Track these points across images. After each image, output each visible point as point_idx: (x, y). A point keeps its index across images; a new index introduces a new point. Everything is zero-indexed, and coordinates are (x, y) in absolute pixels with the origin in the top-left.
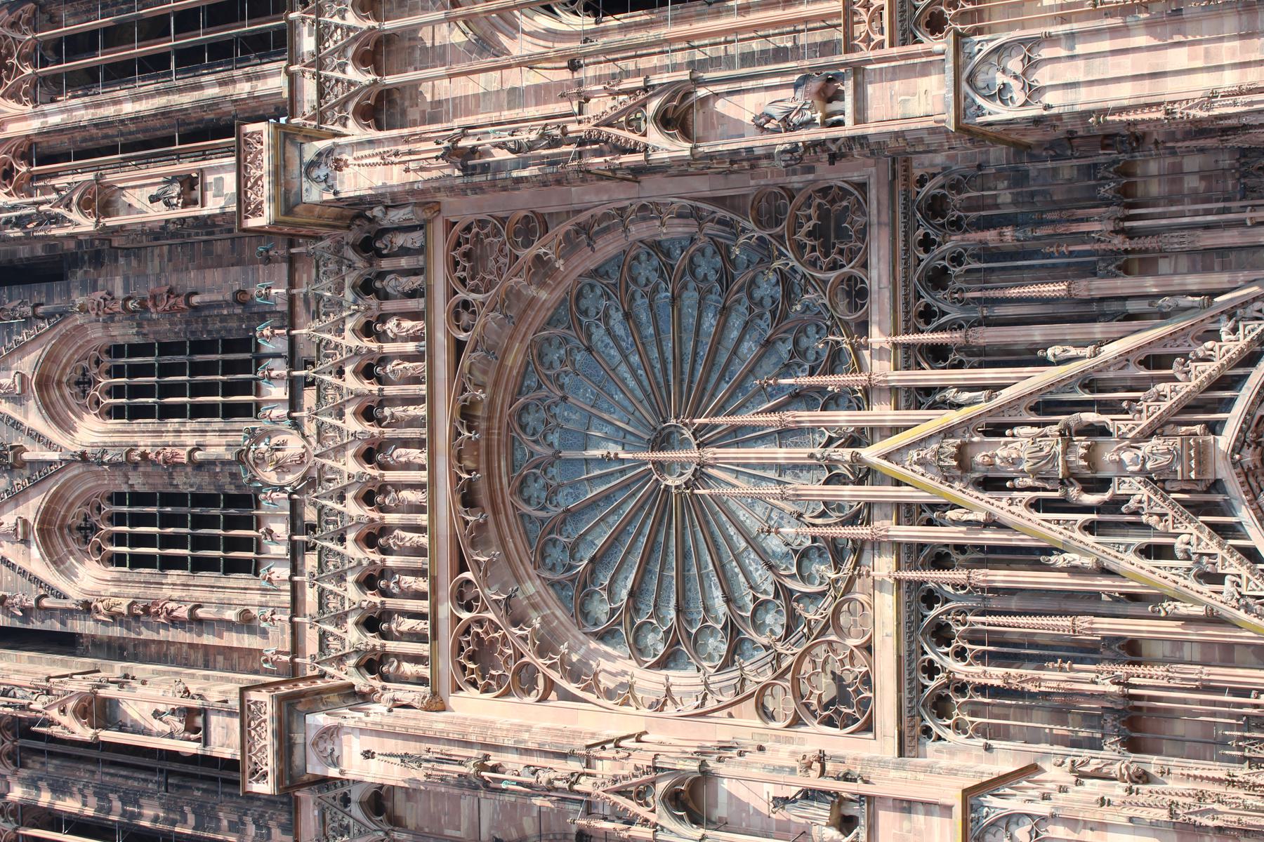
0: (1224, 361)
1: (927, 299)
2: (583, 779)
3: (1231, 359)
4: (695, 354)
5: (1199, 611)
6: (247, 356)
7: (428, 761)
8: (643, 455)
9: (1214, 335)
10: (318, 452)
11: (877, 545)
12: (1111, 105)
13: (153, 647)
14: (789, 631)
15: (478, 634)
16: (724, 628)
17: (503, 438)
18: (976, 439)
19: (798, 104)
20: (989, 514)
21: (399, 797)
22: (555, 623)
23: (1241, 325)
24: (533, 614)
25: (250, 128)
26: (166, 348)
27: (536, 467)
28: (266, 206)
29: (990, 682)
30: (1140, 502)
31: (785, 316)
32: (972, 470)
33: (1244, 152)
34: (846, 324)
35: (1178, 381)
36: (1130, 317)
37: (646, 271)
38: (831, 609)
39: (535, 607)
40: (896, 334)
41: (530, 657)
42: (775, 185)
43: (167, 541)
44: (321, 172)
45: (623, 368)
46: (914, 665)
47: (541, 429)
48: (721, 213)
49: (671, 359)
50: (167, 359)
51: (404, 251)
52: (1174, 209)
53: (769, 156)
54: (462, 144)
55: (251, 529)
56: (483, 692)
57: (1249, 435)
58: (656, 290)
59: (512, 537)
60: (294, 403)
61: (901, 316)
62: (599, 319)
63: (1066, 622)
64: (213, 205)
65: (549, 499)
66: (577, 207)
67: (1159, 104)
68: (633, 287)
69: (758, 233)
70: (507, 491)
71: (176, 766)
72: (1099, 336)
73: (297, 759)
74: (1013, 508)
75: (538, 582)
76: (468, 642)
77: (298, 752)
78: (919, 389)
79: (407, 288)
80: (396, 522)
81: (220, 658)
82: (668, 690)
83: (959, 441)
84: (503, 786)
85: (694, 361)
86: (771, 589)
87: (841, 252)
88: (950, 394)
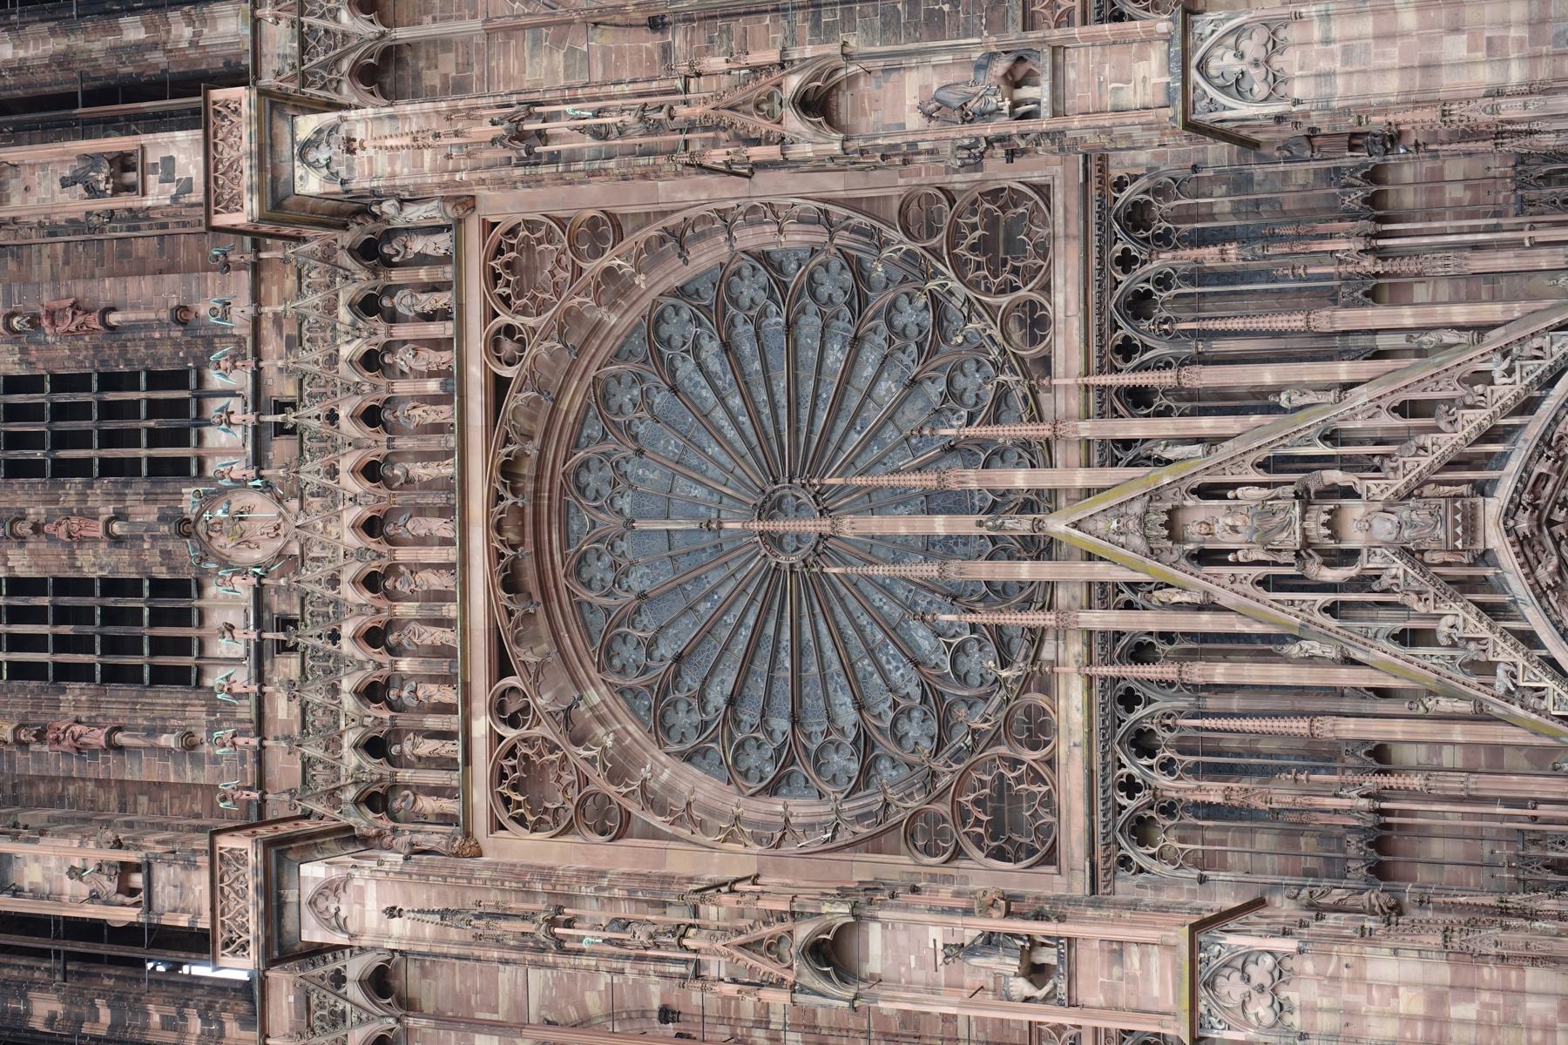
0: (1496, 408)
1: (1126, 330)
2: (692, 932)
3: (1504, 406)
4: (816, 396)
5: (1464, 707)
6: (185, 394)
7: (479, 917)
8: (757, 526)
10: (299, 523)
11: (1061, 633)
12: (1373, 101)
13: (42, 789)
14: (939, 748)
15: (526, 757)
16: (855, 743)
17: (556, 504)
20: (1207, 593)
21: (413, 970)
22: (628, 740)
23: (1517, 364)
24: (600, 731)
25: (218, 94)
26: (62, 383)
28: (246, 197)
29: (1207, 799)
30: (1395, 577)
31: (934, 350)
32: (1185, 541)
33: (1521, 159)
34: (1020, 359)
35: (1442, 431)
36: (1379, 355)
37: (750, 289)
38: (1002, 715)
39: (601, 720)
40: (1087, 374)
41: (600, 783)
43: (62, 644)
44: (322, 155)
45: (719, 415)
46: (1109, 781)
47: (606, 491)
48: (859, 219)
49: (784, 402)
50: (63, 398)
51: (422, 260)
52: (1436, 225)
53: (930, 152)
54: (529, 126)
55: (189, 625)
56: (534, 830)
57: (1525, 496)
58: (763, 313)
59: (568, 631)
60: (258, 460)
61: (1094, 351)
62: (687, 351)
63: (1300, 726)
64: (157, 194)
65: (617, 582)
68: (732, 310)
69: (909, 245)
70: (560, 572)
71: (80, 947)
73: (289, 923)
74: (1236, 586)
75: (603, 689)
76: (514, 768)
79: (428, 308)
80: (413, 612)
81: (143, 800)
82: (787, 820)
83: (1169, 506)
84: (584, 945)
85: (814, 406)
86: (916, 693)
87: (1015, 271)
88: (1158, 451)
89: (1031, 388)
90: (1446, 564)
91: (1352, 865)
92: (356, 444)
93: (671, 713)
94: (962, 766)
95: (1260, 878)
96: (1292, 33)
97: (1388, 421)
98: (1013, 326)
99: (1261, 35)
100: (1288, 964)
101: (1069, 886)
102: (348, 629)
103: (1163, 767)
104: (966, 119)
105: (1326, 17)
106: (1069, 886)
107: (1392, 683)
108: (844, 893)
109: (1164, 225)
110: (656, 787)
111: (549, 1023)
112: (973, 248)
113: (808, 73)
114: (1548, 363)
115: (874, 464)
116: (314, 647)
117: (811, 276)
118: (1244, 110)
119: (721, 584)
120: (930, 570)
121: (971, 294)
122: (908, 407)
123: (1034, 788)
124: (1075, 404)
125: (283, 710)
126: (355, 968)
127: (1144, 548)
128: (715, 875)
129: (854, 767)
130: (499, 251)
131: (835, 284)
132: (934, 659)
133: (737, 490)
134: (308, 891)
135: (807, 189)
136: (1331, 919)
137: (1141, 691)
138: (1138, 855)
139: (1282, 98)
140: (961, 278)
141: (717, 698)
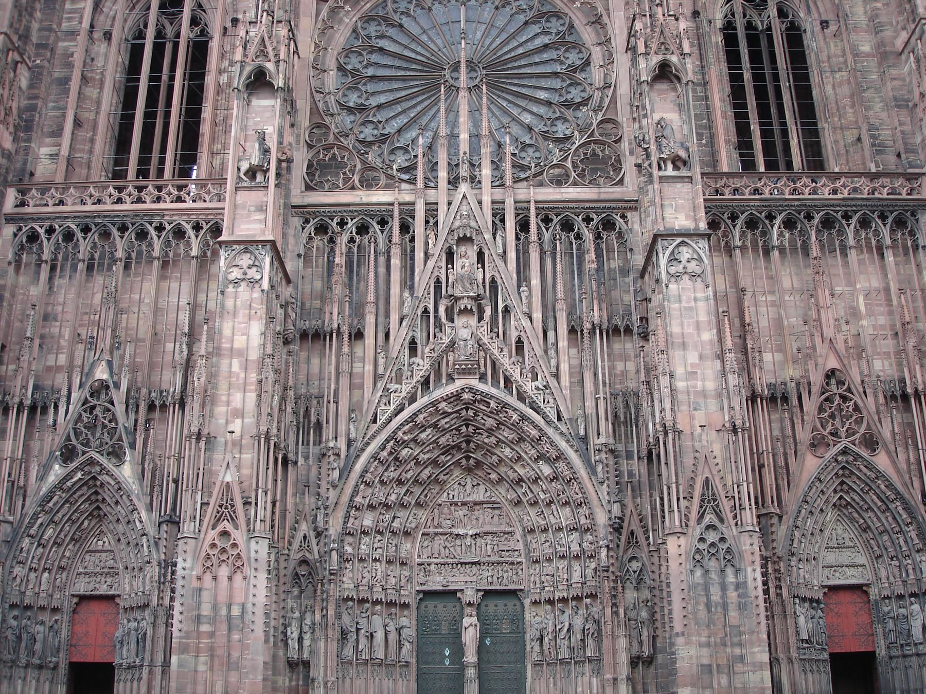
1: (556, 220)
2: (271, 18)
5: (381, 370)
12: (667, 320)
16: (362, 104)
18: (475, 247)
19: (672, 144)
31: (546, 139)
32: (457, 245)
33: (636, 394)
34: (541, 173)
36: (545, 333)
37: (573, 58)
40: (536, 202)
48: (607, 101)
53: (641, 128)
58: (562, 63)
61: (546, 205)
63: (371, 297)
66: (612, 15)
68: (563, 49)
74: (436, 269)
78: (504, 215)
85: (519, 85)
87: (583, 170)
88: (499, 233)
91: (307, 322)
93: (376, 23)
96: (699, 284)
97: (514, 335)
99: (698, 270)
100: (257, 286)
101: (296, 196)
105: (707, 299)
106: (296, 196)
107: (392, 338)
109: (605, 237)
110: (341, 15)
112: (593, 150)
113: (679, 67)
114: (542, 406)
118: (663, 261)
119: (436, 45)
121: (572, 151)
122: (519, 127)
123: (341, 181)
127: (454, 227)
128: (300, 38)
129: (351, 104)
131: (575, 95)
132: (402, 140)
135: (621, 77)
137: (387, 228)
139: (669, 280)
141: (384, 43)
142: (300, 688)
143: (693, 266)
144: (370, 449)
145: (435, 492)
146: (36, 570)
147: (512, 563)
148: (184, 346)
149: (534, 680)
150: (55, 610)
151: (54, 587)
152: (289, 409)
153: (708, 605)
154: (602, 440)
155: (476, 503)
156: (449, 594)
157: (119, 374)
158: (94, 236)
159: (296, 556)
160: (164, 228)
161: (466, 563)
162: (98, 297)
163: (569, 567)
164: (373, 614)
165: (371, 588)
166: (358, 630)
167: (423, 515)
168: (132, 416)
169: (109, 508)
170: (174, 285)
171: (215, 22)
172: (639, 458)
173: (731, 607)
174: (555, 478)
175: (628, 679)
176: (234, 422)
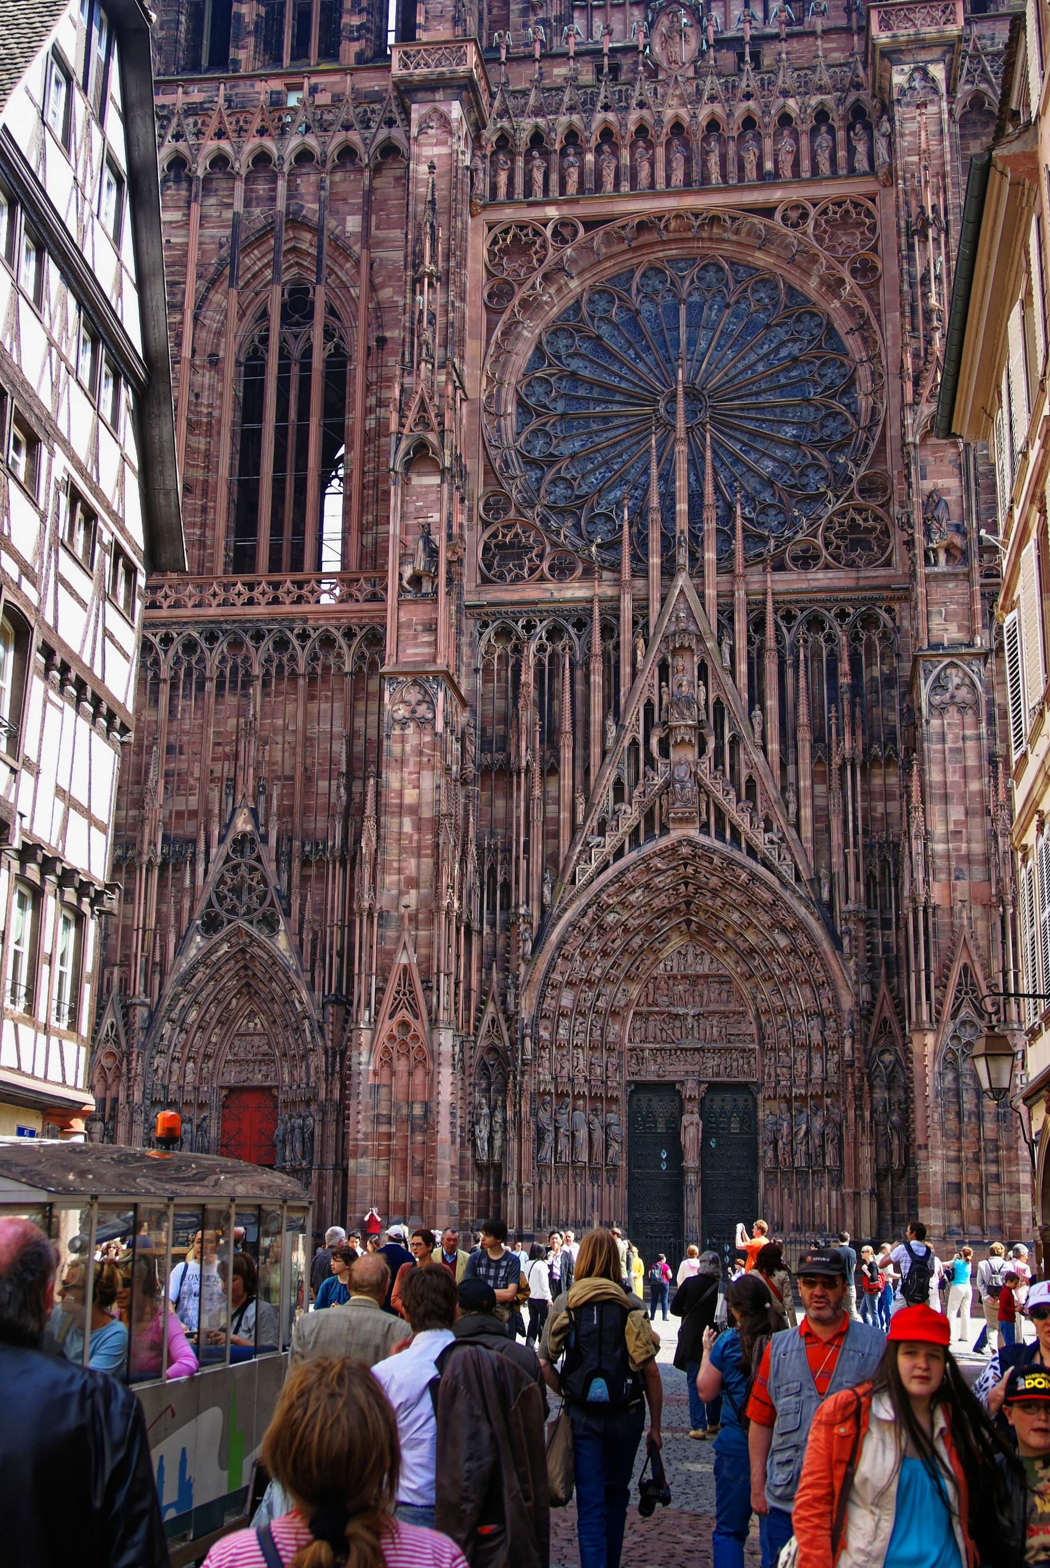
1: (800, 616)
2: (430, 366)
5: (580, 818)
9: (768, 829)
11: (618, 583)
12: (926, 767)
15: (534, 243)
16: (551, 455)
18: (696, 659)
20: (643, 671)
24: (552, 290)
27: (672, 283)
28: (889, 34)
31: (791, 496)
32: (673, 657)
36: (783, 767)
39: (559, 290)
41: (521, 293)
42: (892, 492)
48: (873, 446)
51: (851, 151)
60: (721, 43)
61: (787, 598)
63: (567, 726)
66: (883, 318)
67: (923, 802)
68: (818, 363)
70: (652, 257)
72: (769, 747)
73: (420, 96)
75: (579, 290)
76: (527, 235)
77: (428, 96)
78: (733, 612)
80: (623, 162)
83: (694, 647)
87: (838, 547)
88: (727, 641)
89: (765, 560)
90: (661, 807)
92: (730, 114)
94: (538, 524)
95: (479, 704)
96: (969, 718)
98: (804, 546)
100: (428, 727)
101: (469, 592)
102: (611, 116)
103: (541, 645)
104: (925, 521)
105: (979, 738)
106: (469, 592)
108: (458, 458)
109: (864, 638)
110: (519, 329)
111: (372, 265)
114: (776, 863)
115: (721, 460)
116: (598, 94)
117: (840, 413)
120: (655, 501)
121: (823, 520)
123: (526, 569)
124: (755, 587)
125: (560, 71)
126: (397, 133)
130: (856, 205)
133: (705, 371)
134: (443, 108)
136: (456, 746)
138: (489, 632)
140: (834, 514)
141: (575, 364)
142: (491, 1195)
143: (963, 693)
144: (567, 916)
145: (648, 962)
146: (179, 1060)
147: (744, 1050)
148: (342, 790)
149: (766, 1190)
150: (202, 1106)
151: (201, 1077)
152: (470, 867)
153: (959, 1115)
154: (851, 906)
155: (698, 977)
156: (668, 1088)
157: (266, 825)
158: (222, 646)
159: (482, 1042)
160: (309, 636)
161: (686, 1050)
162: (233, 721)
163: (809, 1058)
164: (574, 1110)
165: (571, 1080)
166: (557, 1129)
167: (635, 990)
168: (285, 877)
169: (261, 985)
170: (325, 706)
171: (358, 346)
172: (898, 928)
173: (988, 1118)
174: (794, 950)
175: (872, 1192)
176: (408, 893)
